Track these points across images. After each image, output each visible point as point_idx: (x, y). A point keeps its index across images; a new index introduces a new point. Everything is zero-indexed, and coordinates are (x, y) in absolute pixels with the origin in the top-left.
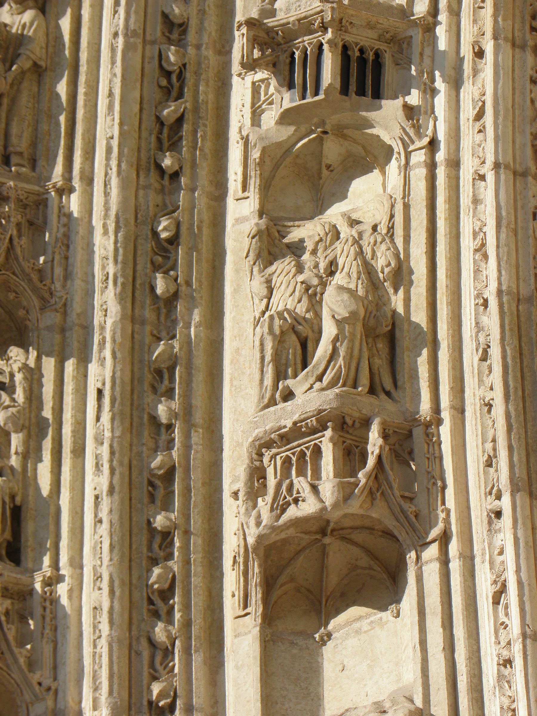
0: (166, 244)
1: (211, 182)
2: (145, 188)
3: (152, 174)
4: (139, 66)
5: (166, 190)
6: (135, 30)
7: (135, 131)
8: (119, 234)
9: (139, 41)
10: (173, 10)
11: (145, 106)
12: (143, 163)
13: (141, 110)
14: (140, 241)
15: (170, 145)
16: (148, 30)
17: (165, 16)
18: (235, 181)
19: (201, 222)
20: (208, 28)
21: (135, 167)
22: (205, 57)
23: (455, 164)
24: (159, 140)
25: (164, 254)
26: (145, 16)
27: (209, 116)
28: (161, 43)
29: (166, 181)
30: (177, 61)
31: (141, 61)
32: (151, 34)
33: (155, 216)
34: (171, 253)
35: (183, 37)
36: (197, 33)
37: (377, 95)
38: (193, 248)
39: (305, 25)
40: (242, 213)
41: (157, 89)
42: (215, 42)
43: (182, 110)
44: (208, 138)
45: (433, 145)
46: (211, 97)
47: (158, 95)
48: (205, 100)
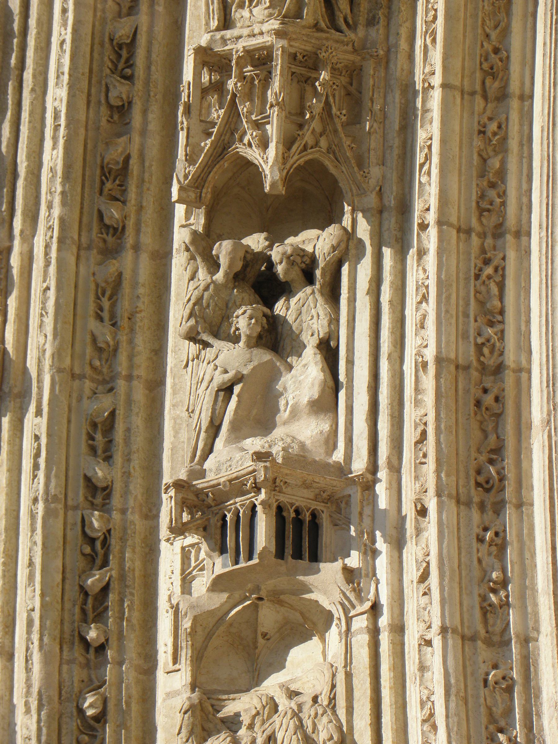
0: (92, 722)
1: (139, 654)
2: (69, 662)
3: (76, 647)
4: (60, 533)
5: (92, 664)
6: (55, 495)
7: (57, 602)
8: (42, 713)
9: (60, 506)
10: (96, 473)
11: (68, 575)
12: (67, 636)
13: (64, 579)
14: (65, 719)
15: (96, 616)
16: (70, 495)
17: (88, 479)
18: (165, 652)
19: (130, 698)
20: (133, 492)
21: (58, 640)
22: (131, 522)
23: (399, 629)
24: (83, 611)
25: (91, 733)
26: (66, 480)
27: (136, 584)
28: (84, 509)
29: (92, 655)
30: (101, 527)
31: (62, 528)
32: (73, 499)
33: (80, 692)
34: (97, 731)
35: (107, 501)
36: (122, 497)
37: (315, 558)
38: (122, 725)
39: (237, 486)
40: (173, 687)
41: (80, 557)
42: (141, 505)
43: (107, 578)
44: (135, 607)
45: (375, 609)
46: (138, 564)
47: (81, 563)
48: (132, 568)
